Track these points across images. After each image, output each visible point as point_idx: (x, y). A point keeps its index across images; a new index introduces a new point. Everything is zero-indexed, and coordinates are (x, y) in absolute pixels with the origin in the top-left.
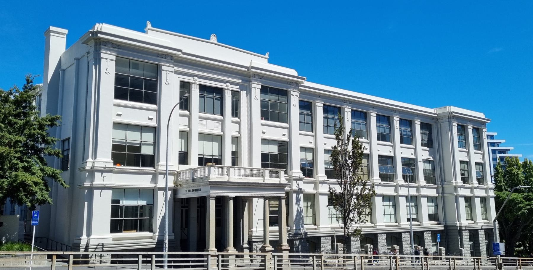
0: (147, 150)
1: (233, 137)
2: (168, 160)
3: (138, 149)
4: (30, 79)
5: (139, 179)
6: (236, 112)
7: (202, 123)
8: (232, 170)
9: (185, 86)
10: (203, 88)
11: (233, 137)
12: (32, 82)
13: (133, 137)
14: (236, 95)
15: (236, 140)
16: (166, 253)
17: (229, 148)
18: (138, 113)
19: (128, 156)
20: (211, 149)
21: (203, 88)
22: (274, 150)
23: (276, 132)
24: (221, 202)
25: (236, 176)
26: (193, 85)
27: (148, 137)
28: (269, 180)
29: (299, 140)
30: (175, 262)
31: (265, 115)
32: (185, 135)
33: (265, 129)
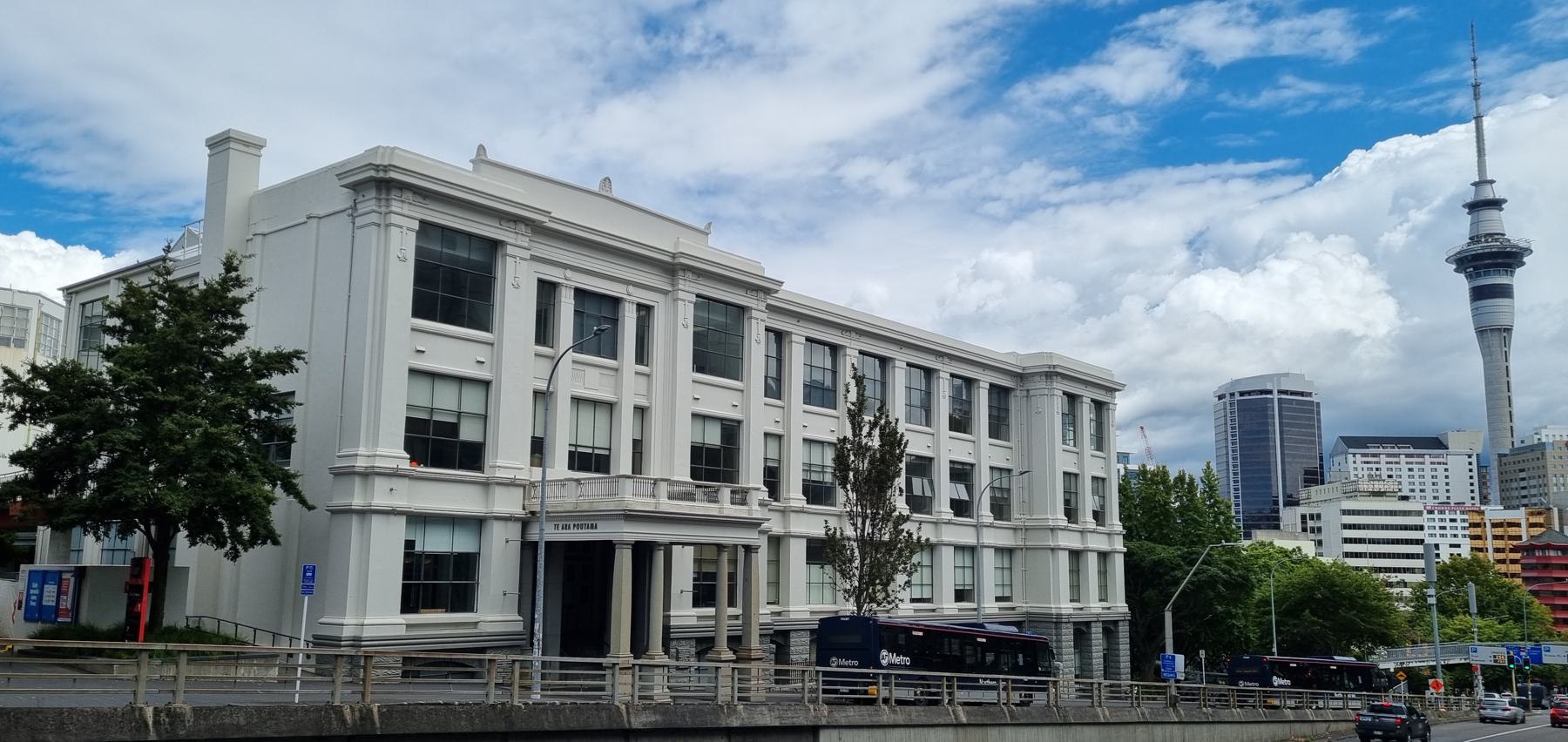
0: (468, 432)
1: (636, 408)
2: (508, 455)
3: (453, 429)
4: (236, 262)
5: (448, 494)
6: (642, 356)
7: (581, 376)
8: (629, 482)
9: (547, 290)
10: (580, 293)
11: (636, 408)
12: (236, 269)
13: (445, 400)
14: (645, 311)
15: (641, 411)
16: (537, 655)
17: (627, 429)
18: (452, 349)
19: (439, 444)
20: (591, 436)
21: (580, 293)
22: (713, 437)
23: (719, 399)
24: (643, 552)
25: (633, 498)
26: (564, 290)
27: (472, 401)
28: (700, 507)
29: (759, 418)
30: (594, 677)
31: (702, 363)
32: (542, 397)
33: (700, 391)
